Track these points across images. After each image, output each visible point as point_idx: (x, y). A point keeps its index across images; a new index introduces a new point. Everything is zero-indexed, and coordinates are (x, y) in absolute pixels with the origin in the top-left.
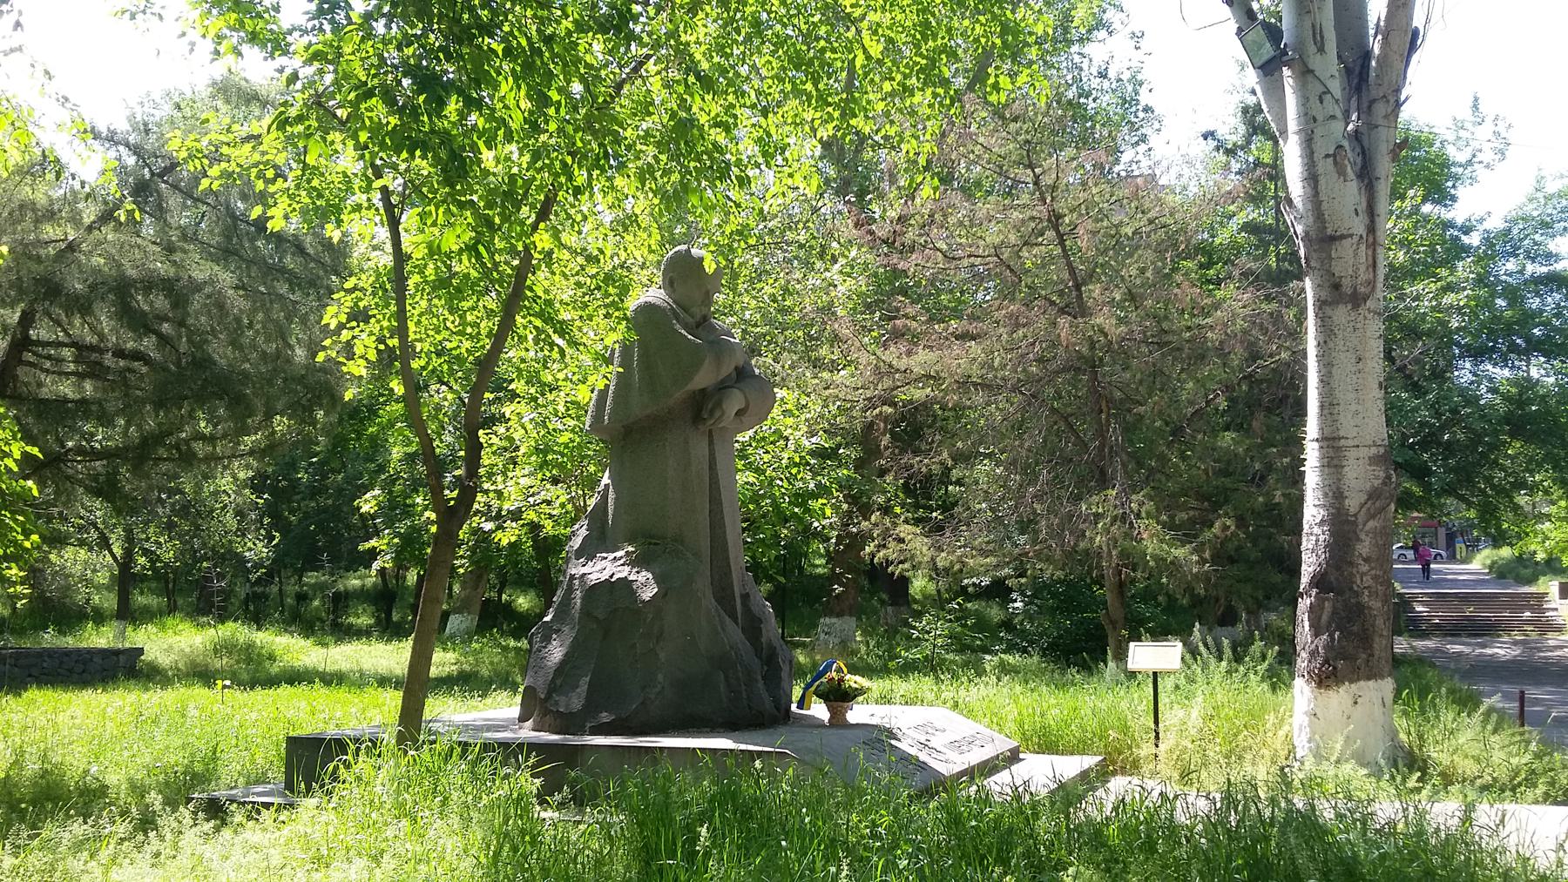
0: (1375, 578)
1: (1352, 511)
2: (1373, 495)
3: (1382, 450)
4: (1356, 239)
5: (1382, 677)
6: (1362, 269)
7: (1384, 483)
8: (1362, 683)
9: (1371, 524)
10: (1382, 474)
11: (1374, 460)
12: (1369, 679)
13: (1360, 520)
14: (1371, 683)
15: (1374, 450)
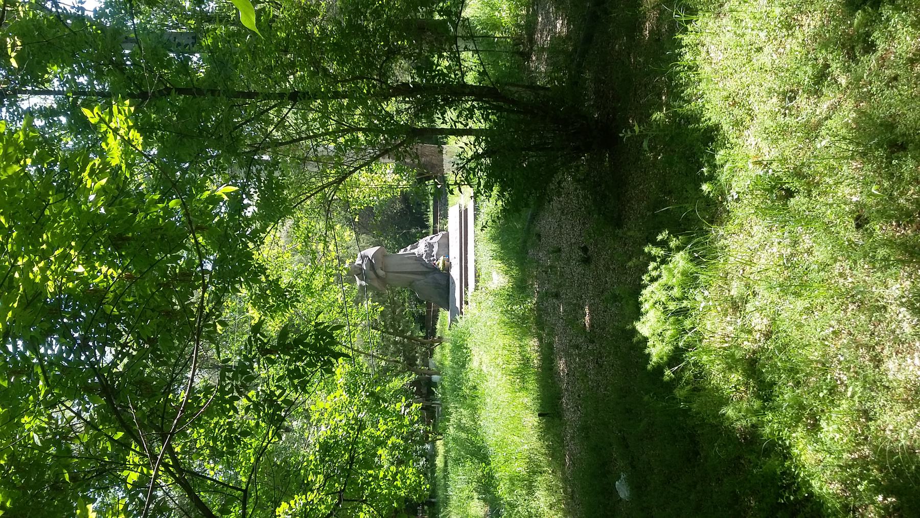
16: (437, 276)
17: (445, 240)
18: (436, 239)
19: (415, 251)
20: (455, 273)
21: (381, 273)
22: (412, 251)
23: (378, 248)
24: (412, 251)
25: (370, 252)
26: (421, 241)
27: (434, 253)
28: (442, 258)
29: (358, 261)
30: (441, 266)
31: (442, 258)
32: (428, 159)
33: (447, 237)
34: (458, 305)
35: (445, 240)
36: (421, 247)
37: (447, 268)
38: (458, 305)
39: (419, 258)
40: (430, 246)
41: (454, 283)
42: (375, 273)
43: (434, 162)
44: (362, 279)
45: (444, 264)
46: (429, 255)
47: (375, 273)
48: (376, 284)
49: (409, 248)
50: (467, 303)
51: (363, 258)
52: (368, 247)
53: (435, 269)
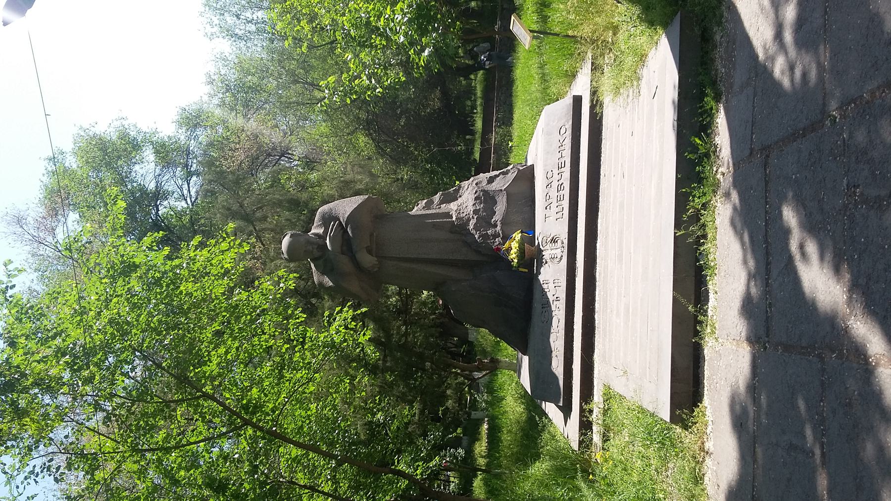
19: (453, 206)
20: (552, 277)
21: (367, 260)
23: (359, 199)
25: (345, 207)
26: (465, 184)
27: (497, 217)
28: (517, 236)
29: (316, 230)
30: (513, 255)
31: (517, 236)
33: (527, 175)
34: (557, 366)
36: (465, 201)
37: (532, 258)
39: (459, 228)
40: (487, 199)
41: (546, 305)
45: (521, 252)
48: (354, 286)
49: (437, 198)
52: (342, 197)
53: (499, 258)
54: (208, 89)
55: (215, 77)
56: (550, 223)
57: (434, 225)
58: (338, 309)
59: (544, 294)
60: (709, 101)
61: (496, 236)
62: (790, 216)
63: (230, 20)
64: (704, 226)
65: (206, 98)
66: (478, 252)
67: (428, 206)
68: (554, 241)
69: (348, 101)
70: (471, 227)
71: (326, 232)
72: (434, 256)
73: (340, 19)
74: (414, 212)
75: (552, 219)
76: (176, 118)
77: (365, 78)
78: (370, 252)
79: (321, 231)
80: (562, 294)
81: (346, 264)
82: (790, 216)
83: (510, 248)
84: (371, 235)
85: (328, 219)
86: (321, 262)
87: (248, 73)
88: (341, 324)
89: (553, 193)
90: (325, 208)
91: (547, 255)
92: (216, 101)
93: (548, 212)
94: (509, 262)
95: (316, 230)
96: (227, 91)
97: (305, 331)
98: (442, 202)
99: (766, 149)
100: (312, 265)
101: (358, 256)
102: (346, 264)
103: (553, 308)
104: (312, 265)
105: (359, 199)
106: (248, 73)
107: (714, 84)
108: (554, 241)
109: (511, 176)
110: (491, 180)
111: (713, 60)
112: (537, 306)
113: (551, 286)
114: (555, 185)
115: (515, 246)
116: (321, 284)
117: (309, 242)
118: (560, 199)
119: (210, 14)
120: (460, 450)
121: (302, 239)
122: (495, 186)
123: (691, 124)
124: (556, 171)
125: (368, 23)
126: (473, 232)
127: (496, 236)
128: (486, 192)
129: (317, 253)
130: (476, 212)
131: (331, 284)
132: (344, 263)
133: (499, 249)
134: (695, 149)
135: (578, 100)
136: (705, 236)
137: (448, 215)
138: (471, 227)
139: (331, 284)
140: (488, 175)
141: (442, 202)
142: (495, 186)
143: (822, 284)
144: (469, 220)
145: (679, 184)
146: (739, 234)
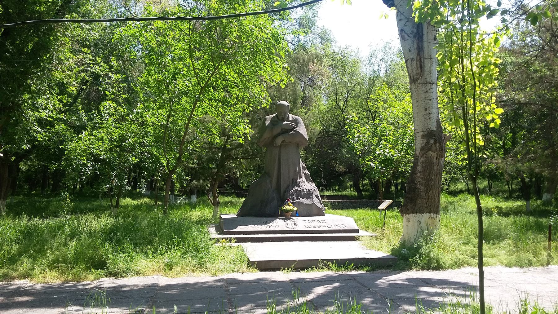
0: (422, 178)
1: (418, 155)
2: (422, 149)
3: (426, 133)
4: (410, 60)
5: (421, 212)
6: (414, 70)
7: (425, 145)
8: (411, 215)
9: (422, 159)
10: (425, 141)
11: (423, 137)
12: (413, 213)
13: (420, 157)
14: (414, 215)
15: (422, 133)
16: (275, 202)
17: (315, 211)
18: (316, 201)
19: (304, 179)
20: (279, 224)
21: (279, 141)
22: (303, 175)
24: (303, 175)
25: (302, 130)
26: (314, 184)
27: (301, 200)
28: (295, 209)
29: (291, 117)
30: (287, 207)
31: (295, 209)
32: (423, 194)
33: (320, 213)
34: (240, 228)
35: (315, 211)
37: (285, 215)
38: (240, 228)
40: (309, 195)
41: (266, 223)
42: (279, 135)
43: (419, 201)
44: (272, 120)
46: (299, 194)
47: (279, 135)
48: (267, 135)
49: (307, 172)
50: (239, 240)
51: (296, 122)
53: (283, 200)
54: (343, 46)
55: (349, 50)
56: (302, 223)
57: (296, 171)
58: (250, 126)
59: (271, 221)
60: (367, 268)
61: (293, 199)
62: (336, 285)
63: (380, 56)
64: (323, 268)
65: (338, 44)
66: (285, 192)
67: (303, 168)
68: (295, 224)
69: (346, 127)
70: (296, 188)
71: (290, 121)
72: (282, 171)
73: (384, 122)
74: (301, 162)
75: (304, 223)
76: (326, 28)
77: (358, 135)
78: (283, 142)
79: (291, 119)
80: (273, 229)
81: (274, 131)
82: (336, 285)
83: (288, 205)
84: (290, 142)
85: (296, 122)
86: (276, 119)
87: (352, 67)
88: (245, 129)
89: (316, 223)
90: (301, 121)
91: (288, 222)
92: (337, 50)
93: (307, 222)
94: (283, 205)
95: (291, 117)
96: (342, 56)
97: (241, 111)
98: (305, 174)
99: (355, 280)
100: (274, 115)
101: (281, 136)
102: (274, 131)
103: (266, 226)
104: (274, 115)
105: (307, 137)
106: (352, 67)
107: (373, 270)
108: (295, 224)
109: (319, 205)
110: (317, 196)
111: (381, 269)
112: (265, 219)
113: (275, 224)
114: (319, 224)
115: (291, 207)
116: (266, 119)
117: (286, 113)
118: (314, 226)
119: (382, 45)
120: (145, 190)
121: (287, 110)
122: (315, 198)
123: (358, 263)
124: (325, 224)
125: (384, 135)
126: (294, 189)
127: (293, 199)
128: (312, 194)
129: (280, 117)
130: (303, 190)
131: (267, 124)
132: (277, 130)
133: (289, 200)
134: (350, 264)
135: (357, 231)
136: (319, 269)
137: (300, 177)
138: (296, 188)
139: (267, 124)
140: (319, 195)
141: (305, 174)
142: (315, 198)
143: (320, 290)
144: (299, 187)
145: (337, 260)
146: (324, 276)
